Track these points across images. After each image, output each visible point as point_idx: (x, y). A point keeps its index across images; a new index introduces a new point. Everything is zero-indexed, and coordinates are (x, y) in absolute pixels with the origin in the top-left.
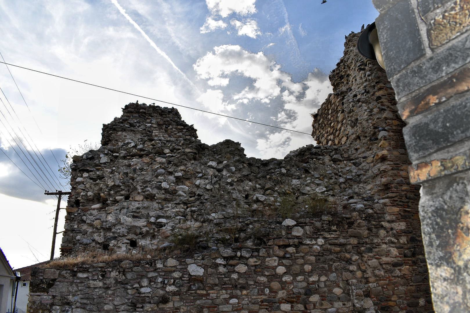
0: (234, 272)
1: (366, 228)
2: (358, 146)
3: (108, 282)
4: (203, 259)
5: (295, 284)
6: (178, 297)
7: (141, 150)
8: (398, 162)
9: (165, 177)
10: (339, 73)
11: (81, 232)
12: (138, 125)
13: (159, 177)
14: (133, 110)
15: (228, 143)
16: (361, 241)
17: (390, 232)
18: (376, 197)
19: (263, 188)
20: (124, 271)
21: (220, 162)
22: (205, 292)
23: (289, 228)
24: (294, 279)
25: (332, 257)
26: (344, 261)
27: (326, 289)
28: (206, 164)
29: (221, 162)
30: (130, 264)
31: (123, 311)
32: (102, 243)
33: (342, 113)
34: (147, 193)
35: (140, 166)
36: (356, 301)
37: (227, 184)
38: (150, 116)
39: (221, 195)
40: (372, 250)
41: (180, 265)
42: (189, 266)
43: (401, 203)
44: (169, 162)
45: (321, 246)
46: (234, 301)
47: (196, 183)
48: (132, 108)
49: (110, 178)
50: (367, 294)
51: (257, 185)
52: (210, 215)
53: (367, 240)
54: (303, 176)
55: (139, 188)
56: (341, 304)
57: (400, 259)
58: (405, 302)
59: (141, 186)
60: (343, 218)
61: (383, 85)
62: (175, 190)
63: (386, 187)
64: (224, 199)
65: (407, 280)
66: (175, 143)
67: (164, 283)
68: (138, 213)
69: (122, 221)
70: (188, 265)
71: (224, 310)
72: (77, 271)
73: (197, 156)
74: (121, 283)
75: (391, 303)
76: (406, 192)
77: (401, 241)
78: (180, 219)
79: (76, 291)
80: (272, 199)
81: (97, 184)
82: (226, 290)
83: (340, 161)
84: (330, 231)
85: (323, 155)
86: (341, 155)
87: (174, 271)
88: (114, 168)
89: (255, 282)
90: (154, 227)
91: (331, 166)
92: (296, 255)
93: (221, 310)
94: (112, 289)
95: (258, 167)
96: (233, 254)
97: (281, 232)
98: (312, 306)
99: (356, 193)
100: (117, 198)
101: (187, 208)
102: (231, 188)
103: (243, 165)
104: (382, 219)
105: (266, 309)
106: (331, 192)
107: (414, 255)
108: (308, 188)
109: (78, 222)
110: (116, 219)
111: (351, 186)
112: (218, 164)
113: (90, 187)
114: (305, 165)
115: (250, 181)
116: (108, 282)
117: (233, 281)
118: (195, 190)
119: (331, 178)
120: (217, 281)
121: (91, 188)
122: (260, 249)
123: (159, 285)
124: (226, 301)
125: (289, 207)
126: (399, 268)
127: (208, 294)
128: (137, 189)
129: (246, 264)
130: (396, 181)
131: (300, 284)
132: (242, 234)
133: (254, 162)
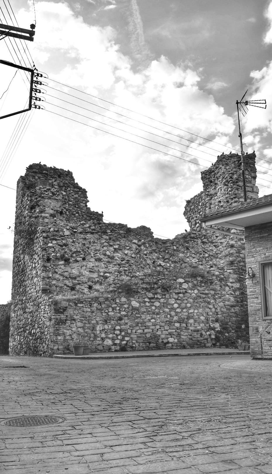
0: (153, 306)
2: (218, 235)
3: (93, 309)
4: (139, 298)
5: (182, 313)
6: (127, 317)
7: (93, 230)
8: (240, 249)
10: (209, 178)
11: (55, 279)
12: (57, 194)
13: (104, 248)
14: (37, 171)
15: (143, 228)
16: (216, 293)
17: (231, 289)
18: (225, 268)
20: (100, 303)
22: (139, 316)
23: (181, 284)
24: (182, 311)
25: (201, 300)
27: (197, 317)
28: (132, 241)
29: (140, 241)
30: (103, 300)
34: (97, 257)
35: (93, 240)
36: (211, 324)
37: (144, 255)
38: (51, 177)
40: (221, 297)
43: (238, 273)
44: (110, 239)
45: (196, 294)
46: (153, 320)
47: (125, 253)
48: (37, 169)
49: (73, 246)
50: (217, 321)
51: (160, 256)
52: (135, 273)
53: (219, 292)
56: (204, 324)
61: (238, 200)
62: (113, 256)
63: (232, 263)
64: (143, 264)
66: (113, 226)
67: (120, 310)
68: (93, 269)
69: (84, 274)
70: (131, 301)
71: (149, 325)
73: (126, 235)
75: (228, 326)
79: (78, 314)
80: (168, 265)
81: (63, 249)
82: (149, 315)
83: (207, 243)
84: (201, 286)
85: (197, 239)
86: (208, 239)
87: (125, 304)
88: (75, 240)
89: (163, 311)
90: (102, 278)
92: (184, 298)
93: (147, 325)
94: (95, 312)
95: (161, 245)
96: (153, 296)
98: (190, 325)
99: (214, 264)
100: (78, 259)
101: (120, 267)
102: (146, 257)
103: (153, 243)
104: (228, 281)
106: (200, 263)
107: (242, 301)
108: (188, 259)
111: (212, 259)
112: (138, 241)
113: (59, 251)
114: (187, 244)
115: (156, 253)
116: (93, 309)
117: (153, 311)
118: (124, 256)
119: (201, 254)
121: (59, 251)
122: (166, 294)
123: (118, 311)
124: (149, 320)
125: (178, 270)
126: (234, 308)
127: (141, 317)
128: (90, 254)
129: (159, 302)
130: (237, 260)
131: (185, 313)
132: (155, 285)
133: (158, 241)
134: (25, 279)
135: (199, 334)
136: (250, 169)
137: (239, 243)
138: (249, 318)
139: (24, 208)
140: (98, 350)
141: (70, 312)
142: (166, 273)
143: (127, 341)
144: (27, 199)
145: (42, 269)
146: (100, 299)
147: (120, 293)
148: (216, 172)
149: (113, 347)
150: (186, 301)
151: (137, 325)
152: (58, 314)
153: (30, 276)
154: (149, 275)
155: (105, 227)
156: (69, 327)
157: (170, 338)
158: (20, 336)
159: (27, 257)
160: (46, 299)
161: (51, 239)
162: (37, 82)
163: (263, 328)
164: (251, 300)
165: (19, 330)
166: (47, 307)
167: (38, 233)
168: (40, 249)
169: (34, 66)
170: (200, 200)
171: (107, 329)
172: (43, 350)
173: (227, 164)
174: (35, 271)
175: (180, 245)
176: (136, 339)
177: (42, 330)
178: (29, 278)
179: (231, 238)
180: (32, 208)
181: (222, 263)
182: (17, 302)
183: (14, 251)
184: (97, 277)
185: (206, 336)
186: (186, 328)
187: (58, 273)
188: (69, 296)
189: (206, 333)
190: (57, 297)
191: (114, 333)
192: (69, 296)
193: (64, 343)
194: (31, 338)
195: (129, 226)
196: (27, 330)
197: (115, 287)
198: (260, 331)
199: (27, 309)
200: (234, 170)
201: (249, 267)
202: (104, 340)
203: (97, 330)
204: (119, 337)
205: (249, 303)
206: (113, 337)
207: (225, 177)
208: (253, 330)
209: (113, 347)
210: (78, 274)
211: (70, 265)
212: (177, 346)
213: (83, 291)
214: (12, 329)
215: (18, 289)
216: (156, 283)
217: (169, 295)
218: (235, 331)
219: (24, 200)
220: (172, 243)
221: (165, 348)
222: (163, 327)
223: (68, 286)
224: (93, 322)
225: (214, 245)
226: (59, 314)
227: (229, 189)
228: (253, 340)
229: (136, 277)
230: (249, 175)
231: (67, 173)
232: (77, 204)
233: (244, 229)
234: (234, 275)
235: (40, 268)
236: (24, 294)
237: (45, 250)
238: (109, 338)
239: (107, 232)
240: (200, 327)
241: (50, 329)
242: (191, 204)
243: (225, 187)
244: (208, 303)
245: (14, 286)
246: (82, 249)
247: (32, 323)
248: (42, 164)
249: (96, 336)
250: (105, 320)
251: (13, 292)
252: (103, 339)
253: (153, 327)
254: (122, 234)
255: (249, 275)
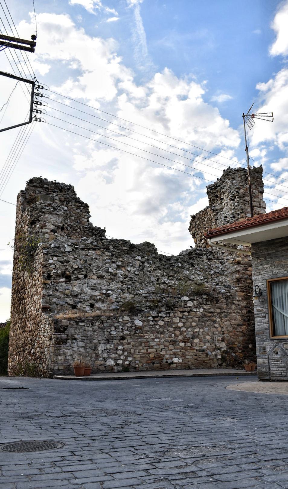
0: (157, 324)
1: (225, 303)
2: (224, 251)
3: (95, 328)
4: (142, 317)
5: (187, 332)
6: (130, 337)
7: (95, 246)
8: (246, 266)
9: (110, 265)
10: (215, 193)
11: (56, 297)
12: (59, 209)
13: (107, 264)
14: (38, 185)
15: (147, 244)
16: (222, 311)
17: (238, 307)
18: (232, 285)
19: (167, 275)
20: (102, 322)
21: (143, 257)
23: (186, 302)
24: (187, 330)
26: (212, 321)
27: (202, 336)
28: (135, 258)
29: (143, 257)
30: (105, 318)
31: (102, 343)
32: (71, 305)
33: (215, 224)
34: (99, 274)
35: (95, 256)
36: (217, 343)
38: (52, 191)
39: (145, 279)
41: (131, 319)
42: (135, 321)
43: (245, 291)
44: (113, 255)
45: (201, 313)
46: (157, 340)
47: (128, 270)
48: (37, 183)
49: (74, 262)
50: (223, 340)
51: (164, 273)
52: (139, 291)
53: (225, 311)
54: (191, 269)
55: (94, 270)
56: (209, 344)
57: (241, 322)
58: (242, 345)
59: (95, 270)
60: (214, 297)
61: (244, 215)
62: (116, 273)
63: (238, 280)
65: (244, 334)
66: (116, 242)
67: (123, 329)
70: (134, 320)
71: (152, 344)
72: (78, 322)
74: (101, 329)
75: (234, 346)
76: (249, 284)
77: (243, 312)
78: (120, 292)
79: (79, 333)
80: (173, 282)
81: (64, 266)
82: (153, 334)
83: (212, 260)
84: (206, 304)
85: (202, 255)
86: (213, 256)
87: (128, 323)
88: (76, 256)
89: (168, 331)
90: (104, 296)
91: (207, 263)
92: (189, 317)
93: (150, 344)
95: (165, 261)
96: (157, 315)
97: (181, 304)
98: (195, 345)
99: (220, 282)
100: (79, 276)
101: (123, 285)
102: (149, 274)
104: (234, 299)
105: (173, 345)
106: (206, 280)
107: (249, 320)
108: (193, 277)
109: (53, 290)
110: (81, 290)
111: (218, 276)
112: (142, 258)
113: (60, 268)
114: (192, 261)
115: (160, 270)
117: (157, 330)
118: (127, 274)
120: (149, 329)
121: (60, 268)
122: (170, 313)
123: (121, 330)
124: (153, 340)
125: (182, 288)
126: (240, 327)
127: (144, 336)
129: (163, 321)
130: (244, 277)
131: (189, 332)
132: (159, 303)
133: (162, 258)
134: (25, 297)
135: (205, 355)
136: (257, 183)
137: (246, 260)
138: (257, 338)
139: (24, 223)
140: (100, 370)
141: (71, 330)
142: (171, 290)
143: (130, 361)
144: (27, 214)
145: (42, 286)
146: (102, 318)
147: (122, 311)
148: (222, 186)
149: (115, 368)
150: (190, 320)
151: (140, 345)
152: (59, 333)
153: (30, 294)
154: (153, 293)
155: (107, 243)
156: (70, 346)
157: (175, 359)
158: (19, 355)
159: (27, 274)
160: (46, 318)
161: (51, 255)
162: (38, 95)
163: (270, 348)
164: (258, 319)
165: (18, 349)
166: (47, 326)
167: (39, 249)
168: (40, 266)
169: (35, 77)
170: (206, 215)
171: (109, 349)
172: (43, 370)
173: (233, 179)
174: (35, 288)
175: (185, 262)
176: (139, 359)
177: (42, 350)
178: (29, 295)
179: (238, 255)
180: (33, 223)
181: (228, 280)
182: (17, 320)
183: (13, 267)
184: (100, 295)
185: (212, 356)
186: (192, 348)
187: (59, 290)
188: (70, 314)
189: (212, 353)
190: (58, 315)
191: (117, 353)
192: (70, 314)
193: (65, 363)
194: (31, 358)
195: (132, 242)
196: (26, 349)
197: (118, 306)
198: (267, 351)
199: (26, 328)
200: (241, 184)
201: (256, 284)
202: (106, 360)
203: (99, 349)
204: (122, 357)
205: (256, 323)
206: (115, 357)
207: (231, 192)
208: (260, 351)
209: (115, 368)
210: (80, 291)
211: (71, 282)
212: (181, 366)
213: (85, 310)
214: (11, 348)
215: (17, 307)
216: (159, 301)
217: (174, 314)
218: (242, 351)
219: (24, 215)
220: (177, 260)
221: (169, 368)
222: (167, 346)
223: (69, 304)
224: (94, 341)
225: (220, 262)
226: (60, 334)
227: (236, 204)
228: (260, 360)
229: (139, 294)
230: (255, 190)
231: (68, 187)
232: (79, 219)
233: (251, 246)
234: (241, 293)
235: (40, 285)
236: (23, 312)
237: (46, 266)
238: (112, 358)
239: (110, 248)
240: (205, 347)
241: (51, 349)
242: (196, 220)
243: (231, 202)
244: (214, 322)
245: (13, 304)
246: (83, 265)
247: (31, 342)
248: (43, 178)
249: (97, 356)
250: (107, 339)
251: (12, 310)
252: (105, 360)
253: (157, 347)
254: (125, 251)
255: (256, 293)
